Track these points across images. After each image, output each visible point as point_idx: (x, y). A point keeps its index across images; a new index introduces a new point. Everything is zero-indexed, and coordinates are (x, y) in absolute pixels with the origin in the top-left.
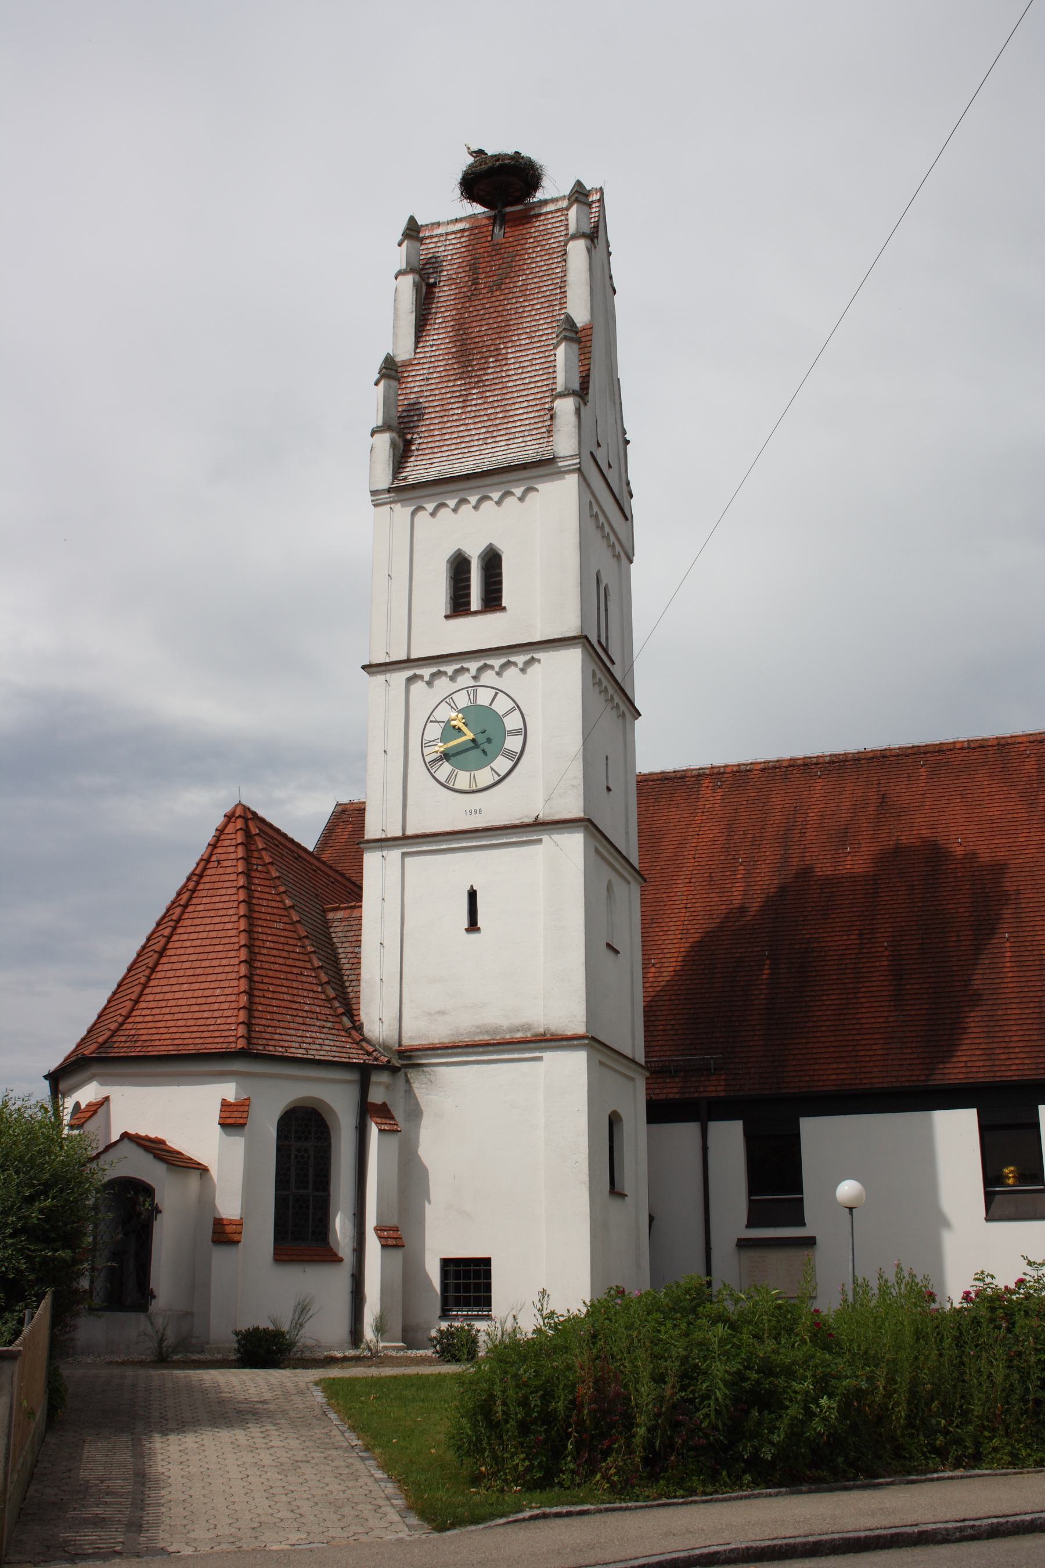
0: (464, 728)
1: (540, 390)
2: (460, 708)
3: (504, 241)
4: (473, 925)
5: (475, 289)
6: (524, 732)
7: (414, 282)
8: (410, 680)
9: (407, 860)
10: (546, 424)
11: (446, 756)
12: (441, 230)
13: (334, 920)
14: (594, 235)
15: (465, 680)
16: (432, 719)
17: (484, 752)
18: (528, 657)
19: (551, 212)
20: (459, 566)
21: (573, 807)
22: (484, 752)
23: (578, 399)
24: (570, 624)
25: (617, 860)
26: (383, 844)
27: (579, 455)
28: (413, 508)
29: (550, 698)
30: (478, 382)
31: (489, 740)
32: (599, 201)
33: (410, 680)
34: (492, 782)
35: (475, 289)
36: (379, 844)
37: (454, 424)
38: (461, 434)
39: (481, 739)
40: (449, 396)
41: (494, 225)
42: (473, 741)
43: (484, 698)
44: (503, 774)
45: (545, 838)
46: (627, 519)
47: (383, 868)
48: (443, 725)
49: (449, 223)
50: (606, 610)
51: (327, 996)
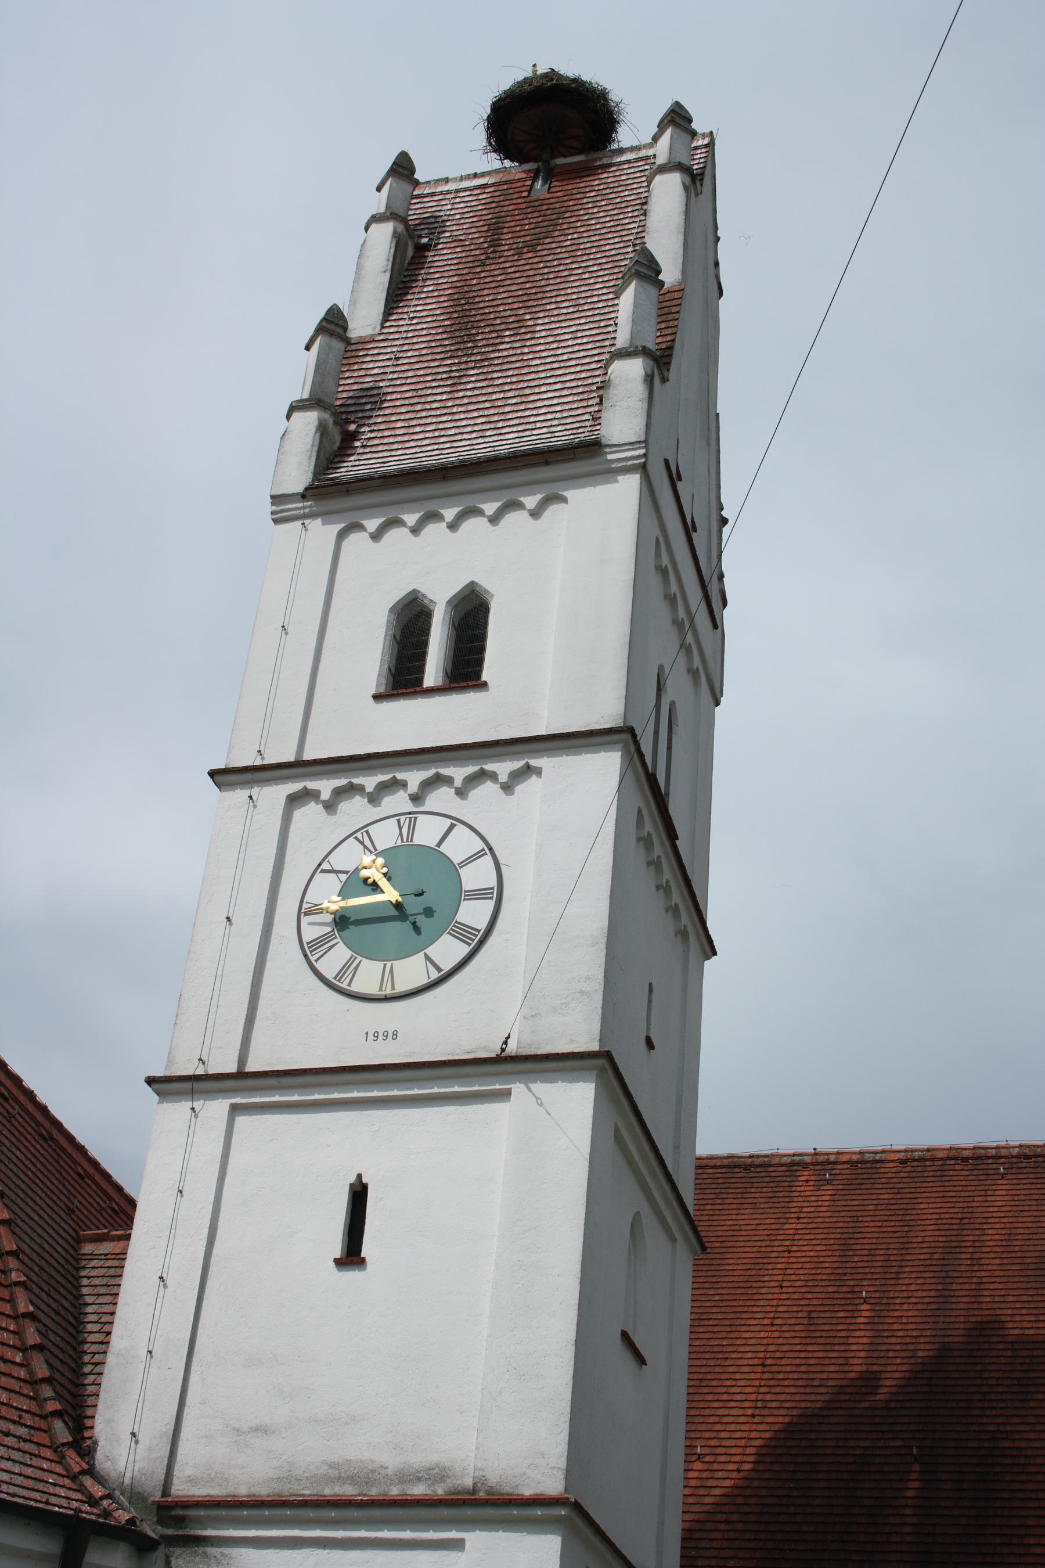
0: (383, 883)
1: (586, 367)
2: (380, 848)
3: (548, 196)
4: (352, 1255)
5: (493, 252)
6: (498, 895)
7: (395, 232)
8: (295, 800)
9: (242, 1121)
10: (592, 409)
11: (342, 921)
12: (451, 186)
13: (93, 1256)
14: (698, 180)
15: (397, 802)
16: (325, 866)
17: (417, 929)
18: (518, 764)
19: (629, 162)
20: (410, 622)
21: (581, 1033)
22: (417, 929)
23: (651, 363)
24: (605, 709)
25: (654, 1177)
26: (197, 1085)
27: (645, 443)
28: (341, 526)
29: (553, 843)
30: (482, 360)
31: (429, 912)
32: (706, 146)
33: (295, 800)
34: (424, 981)
35: (493, 252)
36: (187, 1085)
37: (433, 413)
38: (441, 426)
39: (413, 906)
40: (429, 378)
41: (535, 179)
42: (398, 906)
43: (427, 832)
44: (447, 967)
45: (518, 1089)
46: (715, 626)
47: (190, 1132)
48: (344, 877)
49: (462, 179)
50: (669, 748)
51: (31, 1373)
